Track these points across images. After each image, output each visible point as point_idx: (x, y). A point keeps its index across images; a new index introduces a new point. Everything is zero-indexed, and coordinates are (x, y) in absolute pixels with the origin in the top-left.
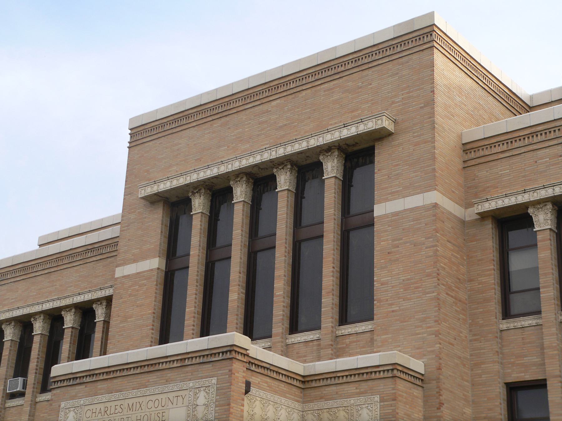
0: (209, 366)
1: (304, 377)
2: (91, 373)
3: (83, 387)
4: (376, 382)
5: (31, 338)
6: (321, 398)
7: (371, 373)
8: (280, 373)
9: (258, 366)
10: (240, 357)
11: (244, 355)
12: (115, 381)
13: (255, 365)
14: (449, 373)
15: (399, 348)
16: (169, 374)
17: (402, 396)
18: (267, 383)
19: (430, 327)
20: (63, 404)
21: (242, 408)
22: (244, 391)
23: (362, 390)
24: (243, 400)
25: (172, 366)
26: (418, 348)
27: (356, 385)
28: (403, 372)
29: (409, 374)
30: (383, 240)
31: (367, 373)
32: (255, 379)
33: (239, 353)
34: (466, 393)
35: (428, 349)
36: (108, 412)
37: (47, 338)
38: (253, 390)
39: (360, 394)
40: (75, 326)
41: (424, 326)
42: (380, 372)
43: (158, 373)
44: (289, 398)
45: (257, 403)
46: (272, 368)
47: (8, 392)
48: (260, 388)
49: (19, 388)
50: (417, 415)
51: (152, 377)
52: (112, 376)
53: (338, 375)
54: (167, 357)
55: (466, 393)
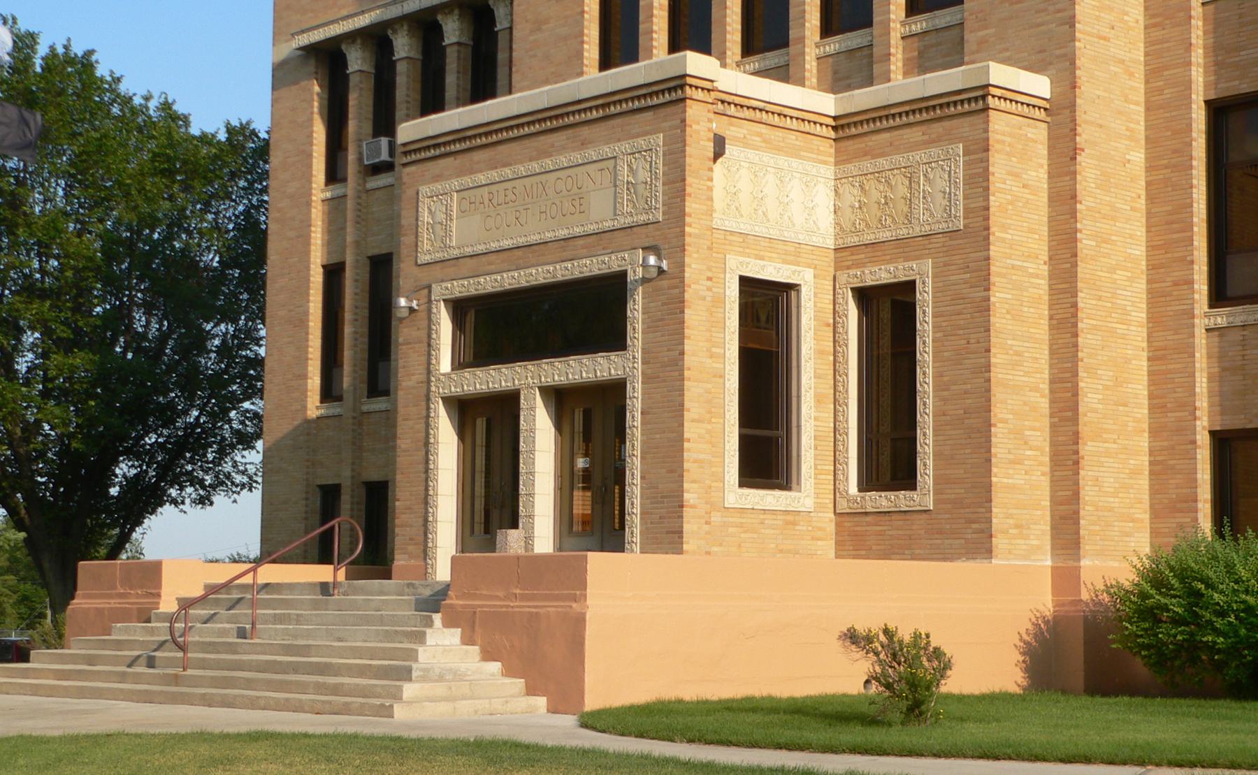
0: (649, 115)
1: (835, 118)
2: (460, 135)
3: (450, 160)
4: (955, 122)
5: (393, 65)
6: (866, 154)
7: (948, 104)
8: (785, 116)
9: (742, 106)
10: (699, 95)
11: (709, 90)
12: (501, 148)
13: (736, 105)
14: (1098, 92)
15: (1008, 54)
16: (585, 132)
17: (1003, 142)
18: (760, 135)
19: (1059, 11)
20: (424, 190)
21: (709, 183)
22: (712, 155)
23: (933, 136)
24: (711, 170)
25: (589, 116)
26: (1040, 52)
27: (924, 128)
28: (1005, 99)
29: (1017, 102)
31: (941, 106)
32: (732, 131)
33: (697, 88)
34: (1132, 125)
35: (1058, 52)
36: (495, 202)
37: (419, 64)
38: (729, 148)
40: (463, 40)
41: (1051, 8)
42: (962, 102)
43: (570, 132)
44: (809, 159)
45: (743, 172)
46: (769, 107)
47: (366, 163)
48: (747, 145)
49: (384, 156)
50: (1034, 174)
52: (494, 138)
53: (893, 111)
54: (579, 102)
55: (1132, 125)
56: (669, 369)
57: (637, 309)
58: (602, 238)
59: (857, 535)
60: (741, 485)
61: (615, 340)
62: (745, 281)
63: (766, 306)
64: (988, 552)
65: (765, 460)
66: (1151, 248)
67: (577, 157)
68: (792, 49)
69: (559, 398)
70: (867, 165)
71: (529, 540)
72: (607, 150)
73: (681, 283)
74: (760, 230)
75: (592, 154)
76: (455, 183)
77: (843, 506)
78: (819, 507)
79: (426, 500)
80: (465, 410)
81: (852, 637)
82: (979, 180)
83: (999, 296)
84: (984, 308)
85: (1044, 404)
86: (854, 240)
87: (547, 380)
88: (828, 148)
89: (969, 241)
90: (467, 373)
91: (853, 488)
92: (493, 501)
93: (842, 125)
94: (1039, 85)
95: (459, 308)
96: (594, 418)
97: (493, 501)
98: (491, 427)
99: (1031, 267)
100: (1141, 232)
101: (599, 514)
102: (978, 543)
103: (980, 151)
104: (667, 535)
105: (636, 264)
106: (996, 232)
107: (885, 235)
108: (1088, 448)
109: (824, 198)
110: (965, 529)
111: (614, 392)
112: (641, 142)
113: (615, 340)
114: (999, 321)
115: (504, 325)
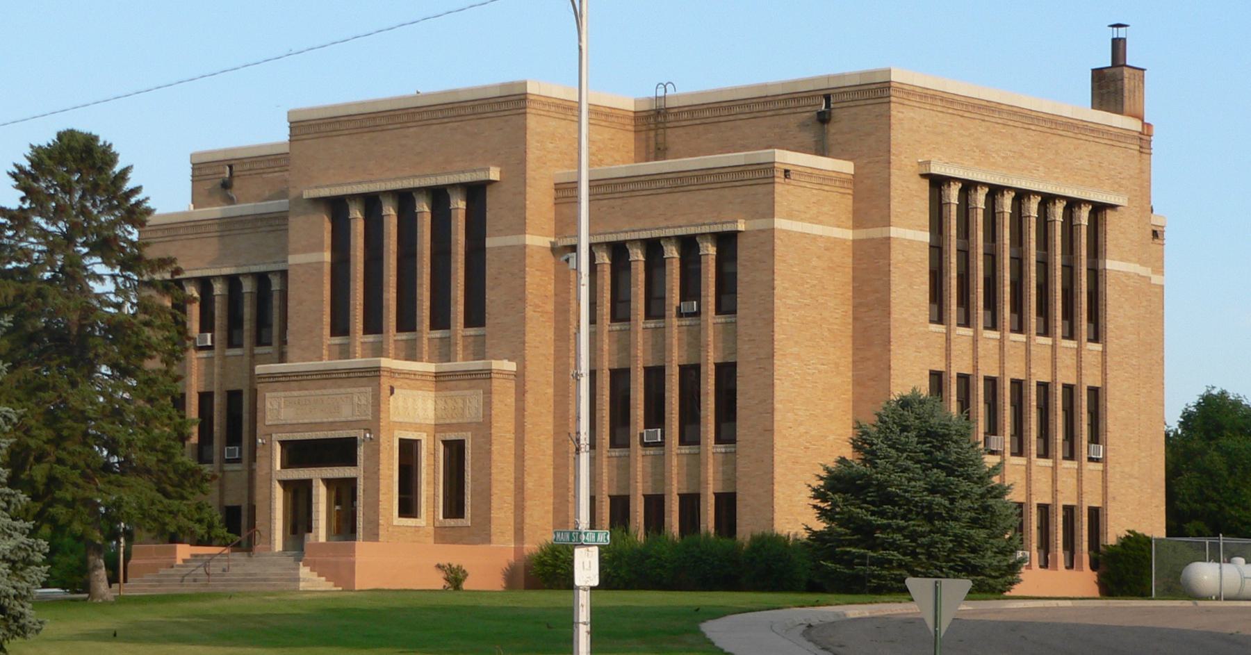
2: (285, 375)
16: (340, 381)
30: (491, 270)
38: (396, 391)
39: (470, 388)
49: (209, 343)
51: (329, 382)
56: (373, 474)
57: (361, 451)
58: (347, 424)
59: (442, 535)
60: (400, 516)
61: (353, 462)
62: (401, 440)
63: (408, 450)
64: (490, 542)
65: (408, 507)
66: (555, 426)
67: (337, 391)
68: (418, 334)
69: (328, 482)
70: (448, 393)
71: (317, 537)
72: (349, 390)
73: (378, 444)
74: (407, 420)
75: (342, 390)
76: (282, 394)
77: (437, 524)
78: (428, 524)
79: (270, 520)
80: (285, 484)
81: (438, 566)
82: (488, 404)
83: (495, 448)
84: (489, 452)
85: (512, 487)
86: (442, 422)
87: (325, 476)
88: (432, 385)
89: (484, 427)
90: (289, 471)
91: (441, 518)
92: (299, 522)
93: (438, 376)
94: (511, 366)
95: (283, 443)
96: (344, 493)
97: (299, 522)
98: (299, 494)
99: (508, 435)
100: (551, 419)
101: (345, 526)
102: (487, 539)
103: (488, 393)
104: (373, 535)
105: (360, 434)
106: (494, 424)
107: (454, 421)
108: (528, 503)
109: (430, 405)
110: (481, 533)
111: (353, 481)
112: (363, 389)
113: (353, 462)
114: (495, 456)
115: (301, 453)
